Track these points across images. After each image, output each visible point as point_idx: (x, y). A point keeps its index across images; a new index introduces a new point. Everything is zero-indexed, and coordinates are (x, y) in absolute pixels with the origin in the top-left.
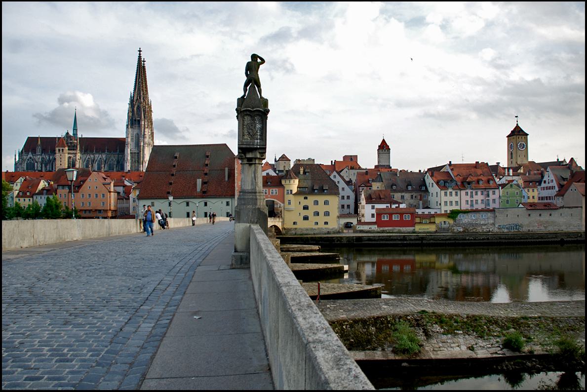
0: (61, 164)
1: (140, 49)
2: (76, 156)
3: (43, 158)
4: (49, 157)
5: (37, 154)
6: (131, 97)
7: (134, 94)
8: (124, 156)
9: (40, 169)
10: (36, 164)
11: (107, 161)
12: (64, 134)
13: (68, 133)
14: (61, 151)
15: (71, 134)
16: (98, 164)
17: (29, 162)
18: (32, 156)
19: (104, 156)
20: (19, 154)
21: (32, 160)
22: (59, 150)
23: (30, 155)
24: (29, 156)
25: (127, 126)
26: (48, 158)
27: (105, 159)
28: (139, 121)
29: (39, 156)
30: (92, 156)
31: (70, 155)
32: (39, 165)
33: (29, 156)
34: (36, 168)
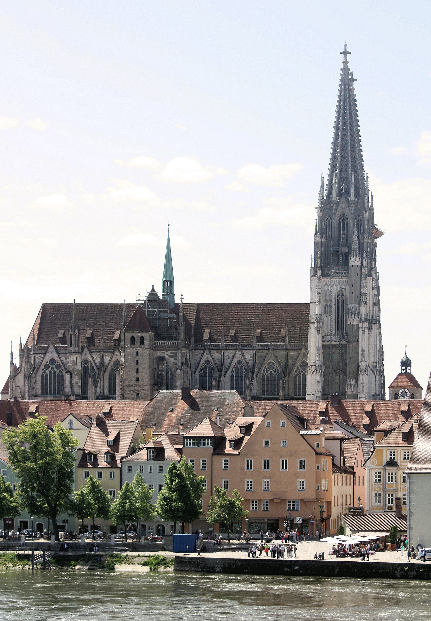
0: (138, 379)
1: (346, 45)
2: (176, 354)
3: (86, 361)
4: (102, 357)
5: (70, 349)
6: (322, 187)
7: (331, 181)
8: (305, 356)
9: (77, 390)
10: (67, 377)
11: (256, 370)
12: (144, 297)
13: (153, 294)
14: (137, 343)
15: (160, 293)
16: (232, 376)
17: (48, 372)
18: (55, 356)
19: (249, 355)
20: (22, 351)
21: (58, 367)
22: (133, 340)
23: (52, 354)
24: (48, 357)
25: (314, 270)
26: (98, 360)
27: (251, 363)
28: (346, 257)
29: (74, 357)
30: (217, 355)
31: (160, 353)
32: (77, 380)
33: (48, 357)
34: (67, 389)
